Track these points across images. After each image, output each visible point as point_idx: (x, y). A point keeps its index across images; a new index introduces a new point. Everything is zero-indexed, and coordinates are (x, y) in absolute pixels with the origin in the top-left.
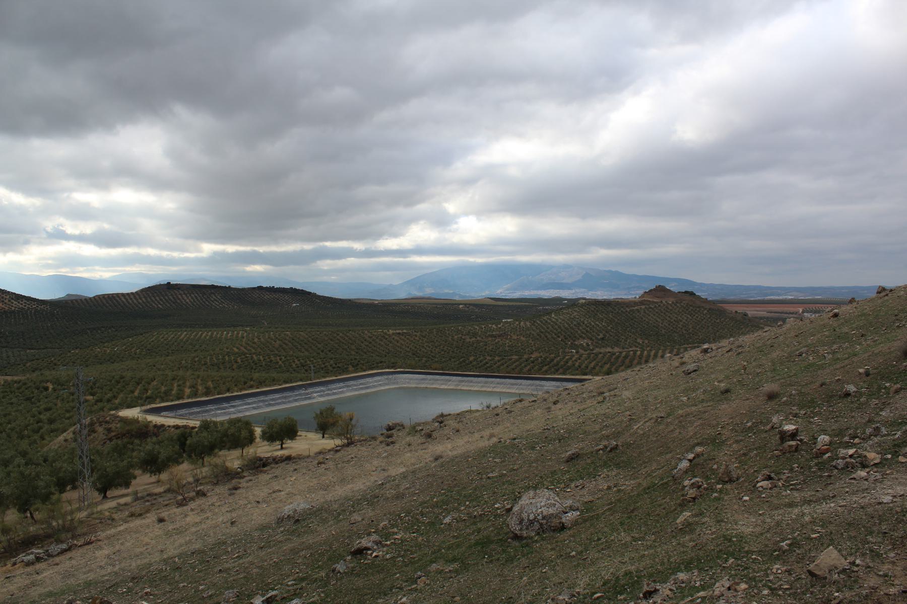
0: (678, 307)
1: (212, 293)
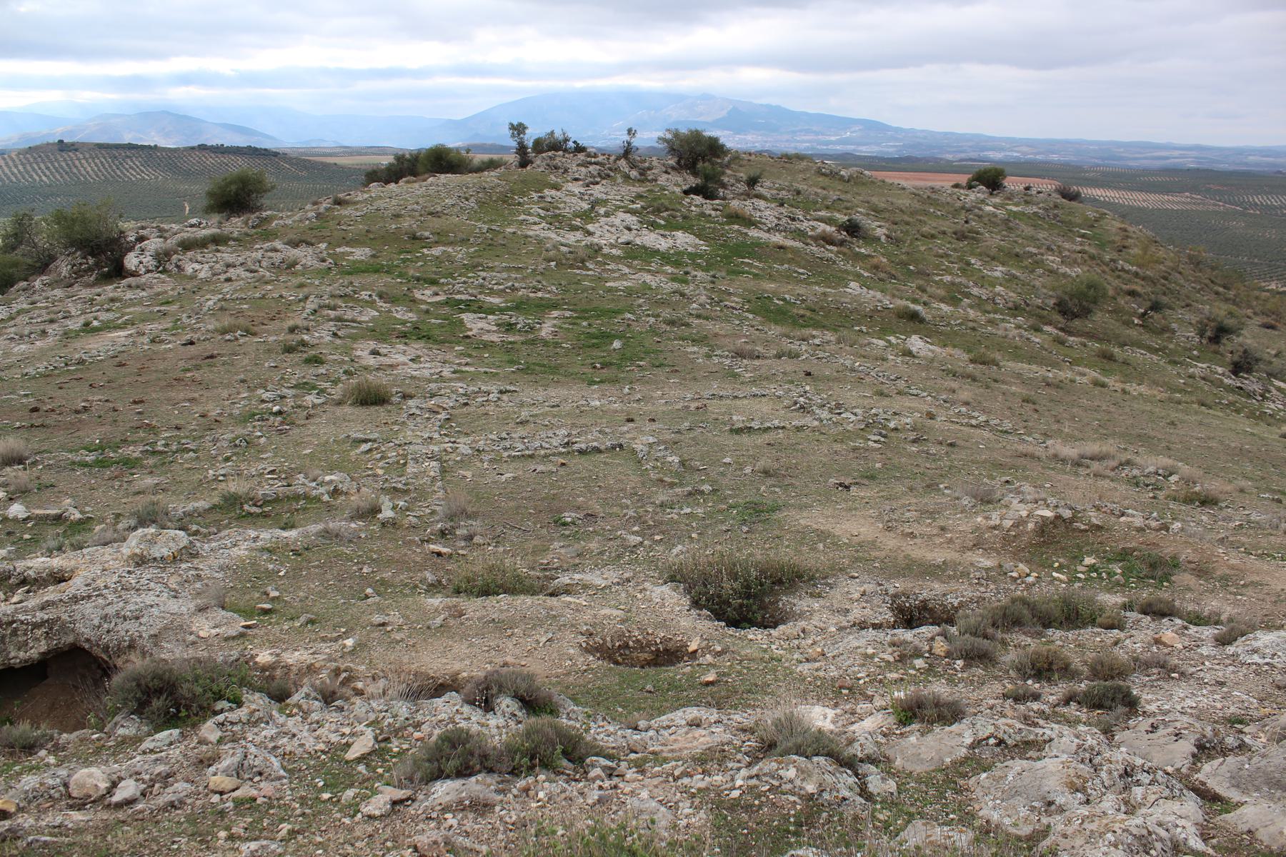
1: (128, 157)
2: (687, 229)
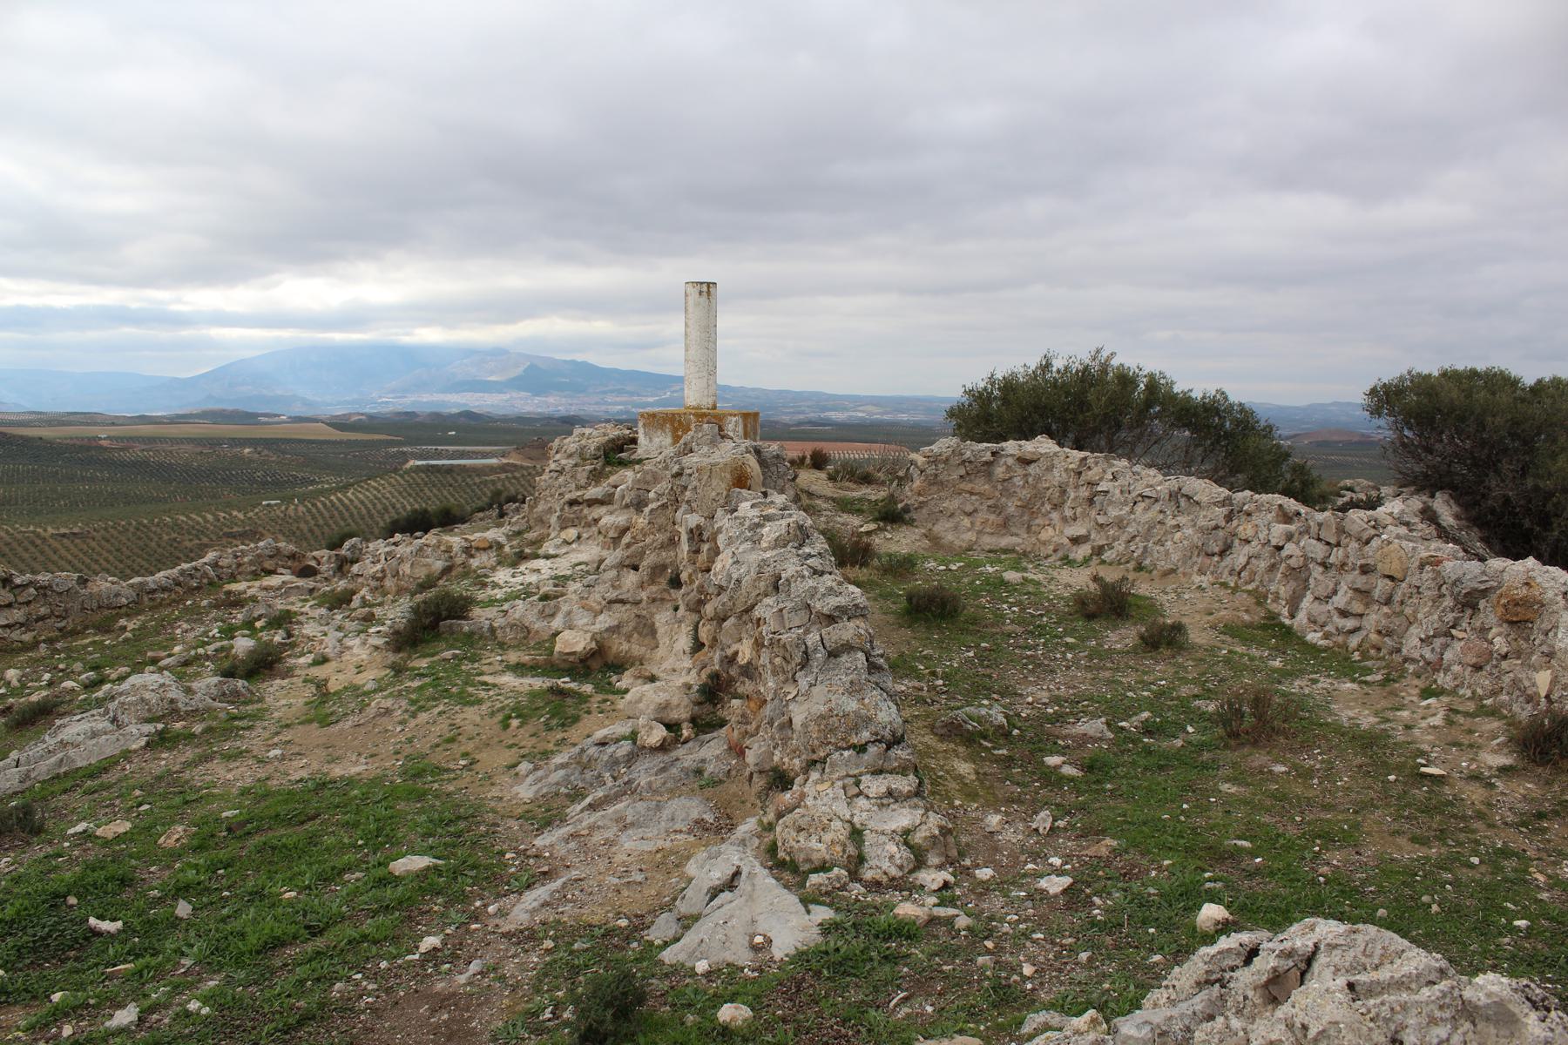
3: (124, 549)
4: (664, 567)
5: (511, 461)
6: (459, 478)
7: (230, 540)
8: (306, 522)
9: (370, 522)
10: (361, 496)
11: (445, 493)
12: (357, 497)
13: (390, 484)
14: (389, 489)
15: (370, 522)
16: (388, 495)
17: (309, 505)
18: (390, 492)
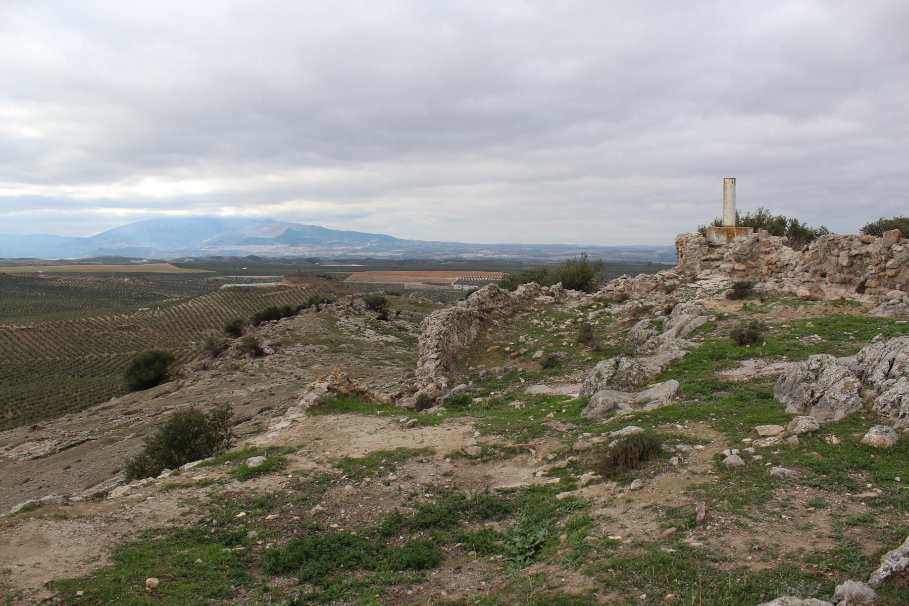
0: (310, 292)
2: (391, 334)
3: (59, 337)
4: (817, 271)
5: (283, 284)
6: (253, 294)
7: (121, 331)
8: (165, 321)
9: (202, 320)
10: (196, 305)
11: (245, 303)
12: (194, 306)
13: (213, 298)
14: (212, 301)
15: (202, 320)
16: (212, 304)
17: (166, 311)
18: (213, 303)
